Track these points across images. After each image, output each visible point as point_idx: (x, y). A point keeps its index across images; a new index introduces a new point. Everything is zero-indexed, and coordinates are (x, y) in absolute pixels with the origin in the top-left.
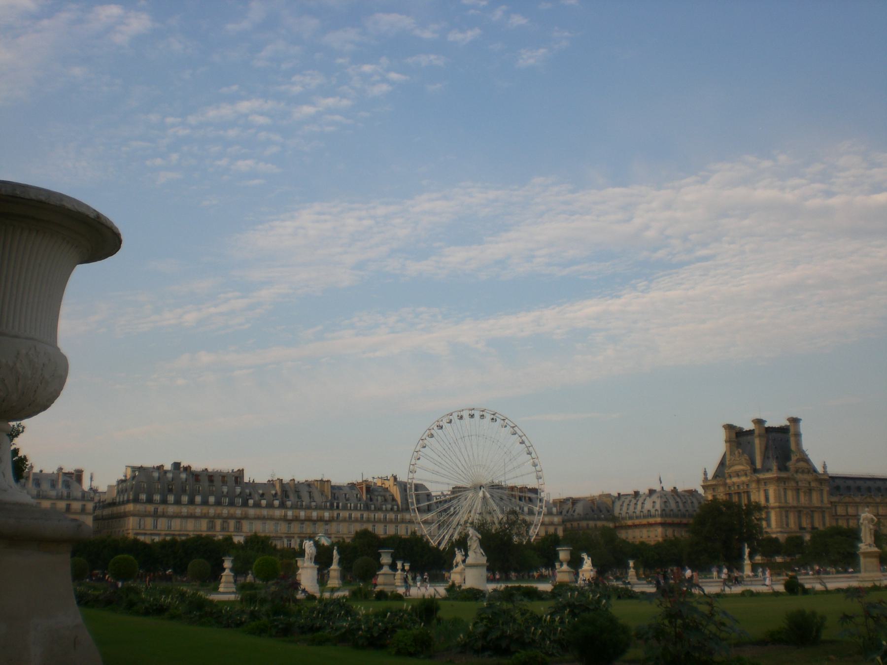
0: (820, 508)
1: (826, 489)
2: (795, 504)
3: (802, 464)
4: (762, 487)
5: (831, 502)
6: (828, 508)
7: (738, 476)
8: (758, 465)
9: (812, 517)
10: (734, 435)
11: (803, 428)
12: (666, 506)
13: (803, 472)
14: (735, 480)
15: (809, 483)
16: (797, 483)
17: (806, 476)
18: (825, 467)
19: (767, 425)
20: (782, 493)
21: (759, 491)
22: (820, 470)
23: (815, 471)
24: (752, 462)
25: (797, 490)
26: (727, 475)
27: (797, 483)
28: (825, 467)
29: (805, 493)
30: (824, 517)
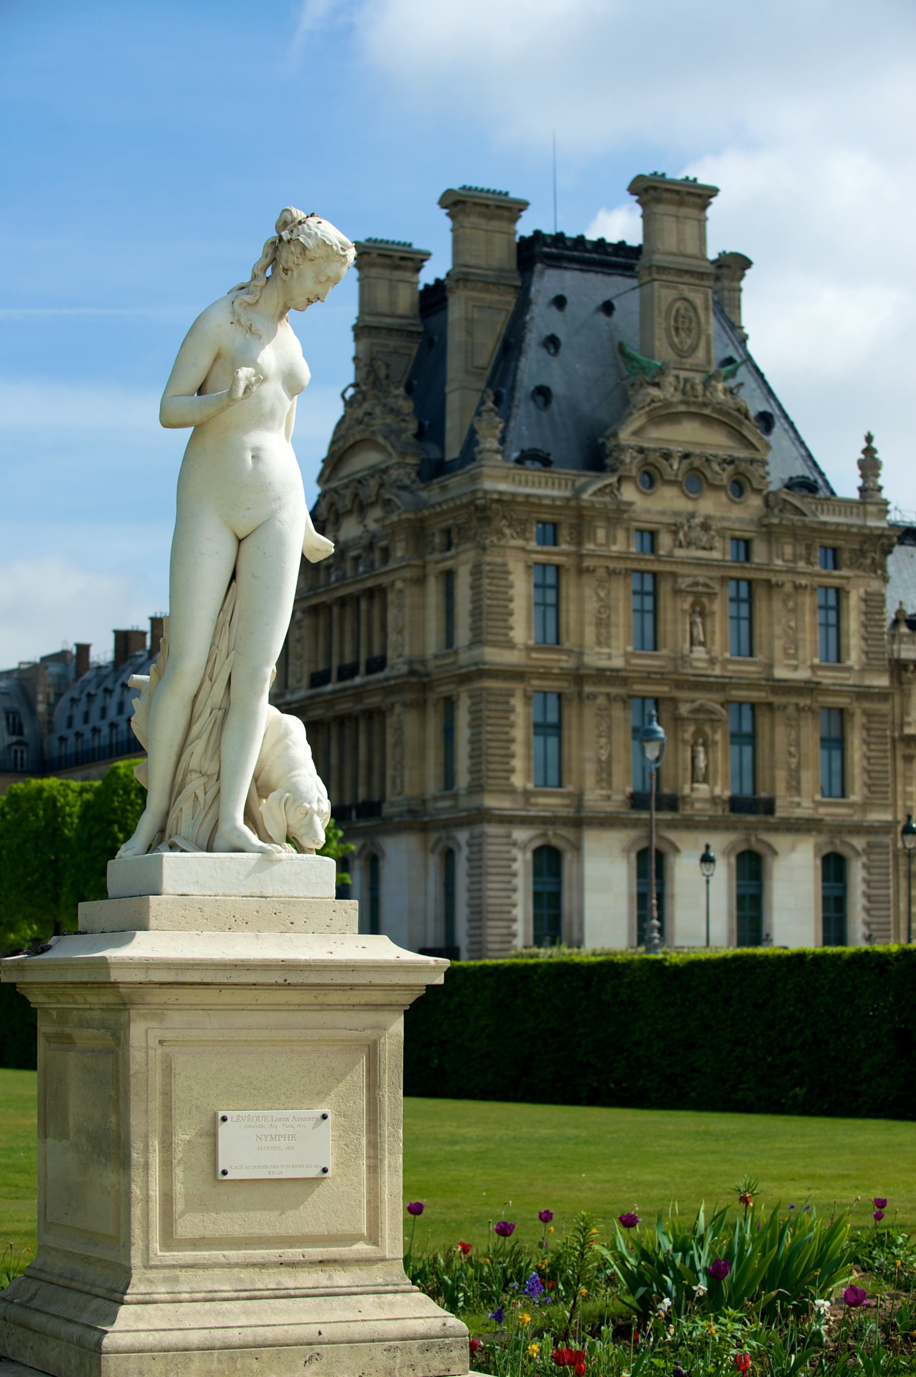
2: (614, 654)
3: (688, 435)
4: (436, 562)
6: (864, 694)
7: (361, 508)
9: (747, 739)
13: (696, 479)
18: (869, 464)
19: (525, 228)
20: (521, 588)
21: (420, 581)
22: (845, 483)
23: (810, 485)
24: (430, 429)
25: (652, 587)
28: (869, 464)
30: (836, 743)
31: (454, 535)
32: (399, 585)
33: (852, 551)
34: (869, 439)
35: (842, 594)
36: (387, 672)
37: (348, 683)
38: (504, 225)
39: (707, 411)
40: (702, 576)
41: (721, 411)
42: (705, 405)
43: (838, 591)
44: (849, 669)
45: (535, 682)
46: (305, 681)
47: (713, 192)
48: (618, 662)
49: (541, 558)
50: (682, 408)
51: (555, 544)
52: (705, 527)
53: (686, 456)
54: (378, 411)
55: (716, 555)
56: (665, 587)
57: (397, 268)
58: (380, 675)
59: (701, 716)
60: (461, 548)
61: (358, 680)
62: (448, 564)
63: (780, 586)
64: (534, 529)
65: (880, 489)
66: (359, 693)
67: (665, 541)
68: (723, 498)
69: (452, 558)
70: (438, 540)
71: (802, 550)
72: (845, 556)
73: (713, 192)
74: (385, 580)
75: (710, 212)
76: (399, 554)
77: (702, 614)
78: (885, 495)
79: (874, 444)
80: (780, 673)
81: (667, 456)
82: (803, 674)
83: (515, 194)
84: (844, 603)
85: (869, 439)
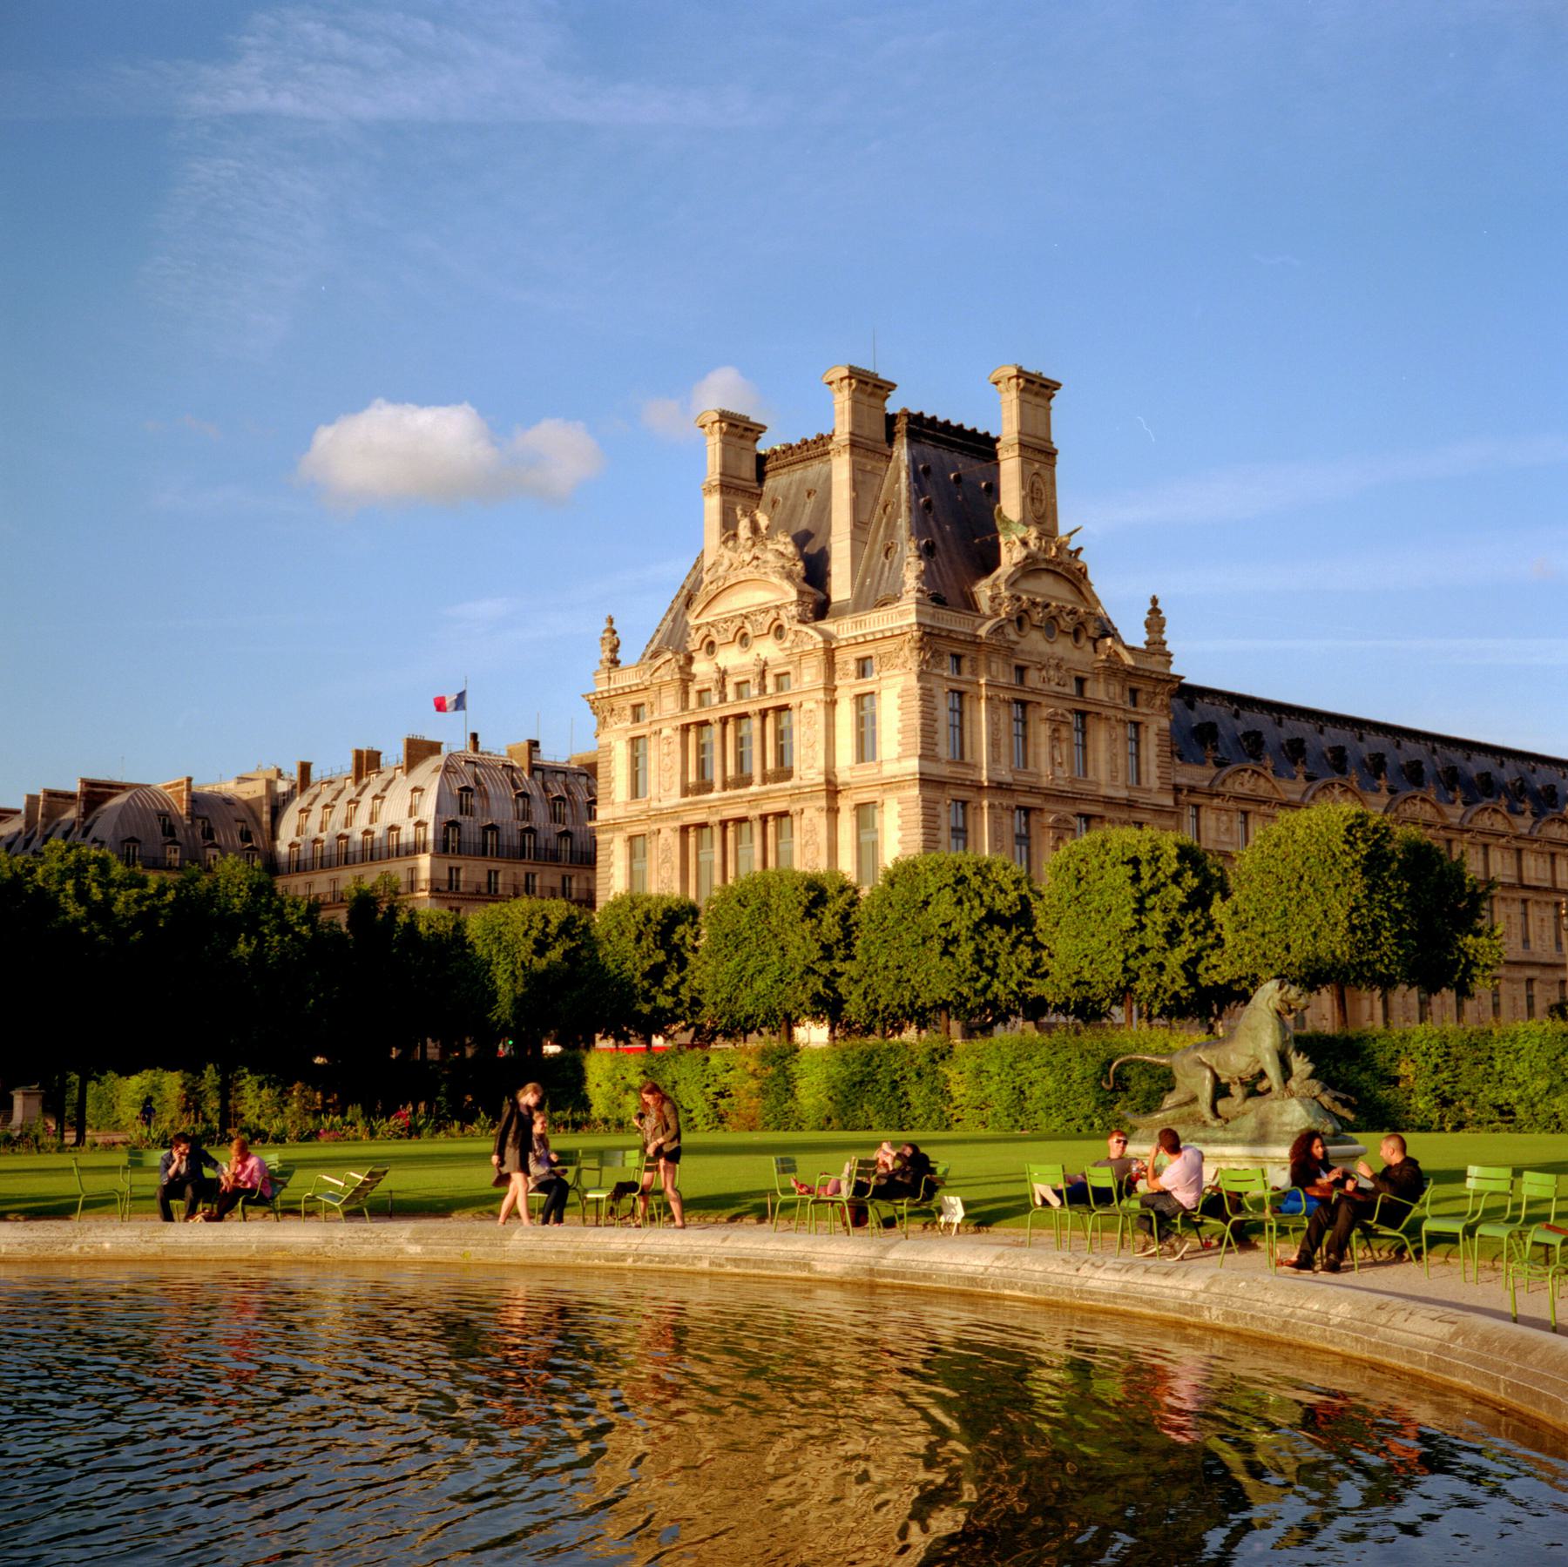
0: (1131, 805)
1: (1158, 723)
5: (1177, 789)
8: (841, 587)
10: (748, 469)
11: (1066, 424)
12: (465, 810)
13: (1050, 626)
14: (731, 658)
15: (1080, 682)
16: (1021, 670)
17: (1062, 647)
18: (1155, 620)
19: (893, 406)
22: (1134, 634)
24: (815, 572)
26: (694, 642)
27: (1021, 670)
28: (1155, 620)
29: (1056, 723)
31: (875, 661)
32: (806, 706)
33: (1148, 693)
34: (1155, 601)
35: (1142, 729)
36: (795, 781)
37: (741, 792)
38: (874, 401)
39: (1059, 570)
40: (1062, 707)
41: (1068, 570)
42: (1059, 564)
43: (1137, 725)
44: (1150, 790)
45: (953, 792)
46: (677, 789)
47: (1057, 386)
48: (1008, 778)
49: (954, 686)
50: (1043, 566)
51: (959, 673)
52: (1058, 667)
53: (1047, 606)
54: (770, 557)
55: (1067, 690)
56: (1033, 716)
57: (742, 437)
58: (787, 784)
59: (1063, 825)
60: (884, 674)
61: (754, 789)
62: (868, 689)
63: (1108, 719)
64: (948, 660)
65: (1164, 643)
66: (754, 800)
67: (1033, 678)
68: (1069, 641)
69: (872, 683)
70: (852, 667)
71: (1118, 689)
72: (1142, 697)
73: (1057, 386)
74: (793, 702)
75: (1053, 402)
76: (807, 679)
77: (1058, 739)
78: (1168, 648)
79: (1159, 606)
80: (1111, 793)
81: (1034, 604)
82: (1123, 794)
83: (884, 375)
84: (1143, 736)
85: (1155, 601)
